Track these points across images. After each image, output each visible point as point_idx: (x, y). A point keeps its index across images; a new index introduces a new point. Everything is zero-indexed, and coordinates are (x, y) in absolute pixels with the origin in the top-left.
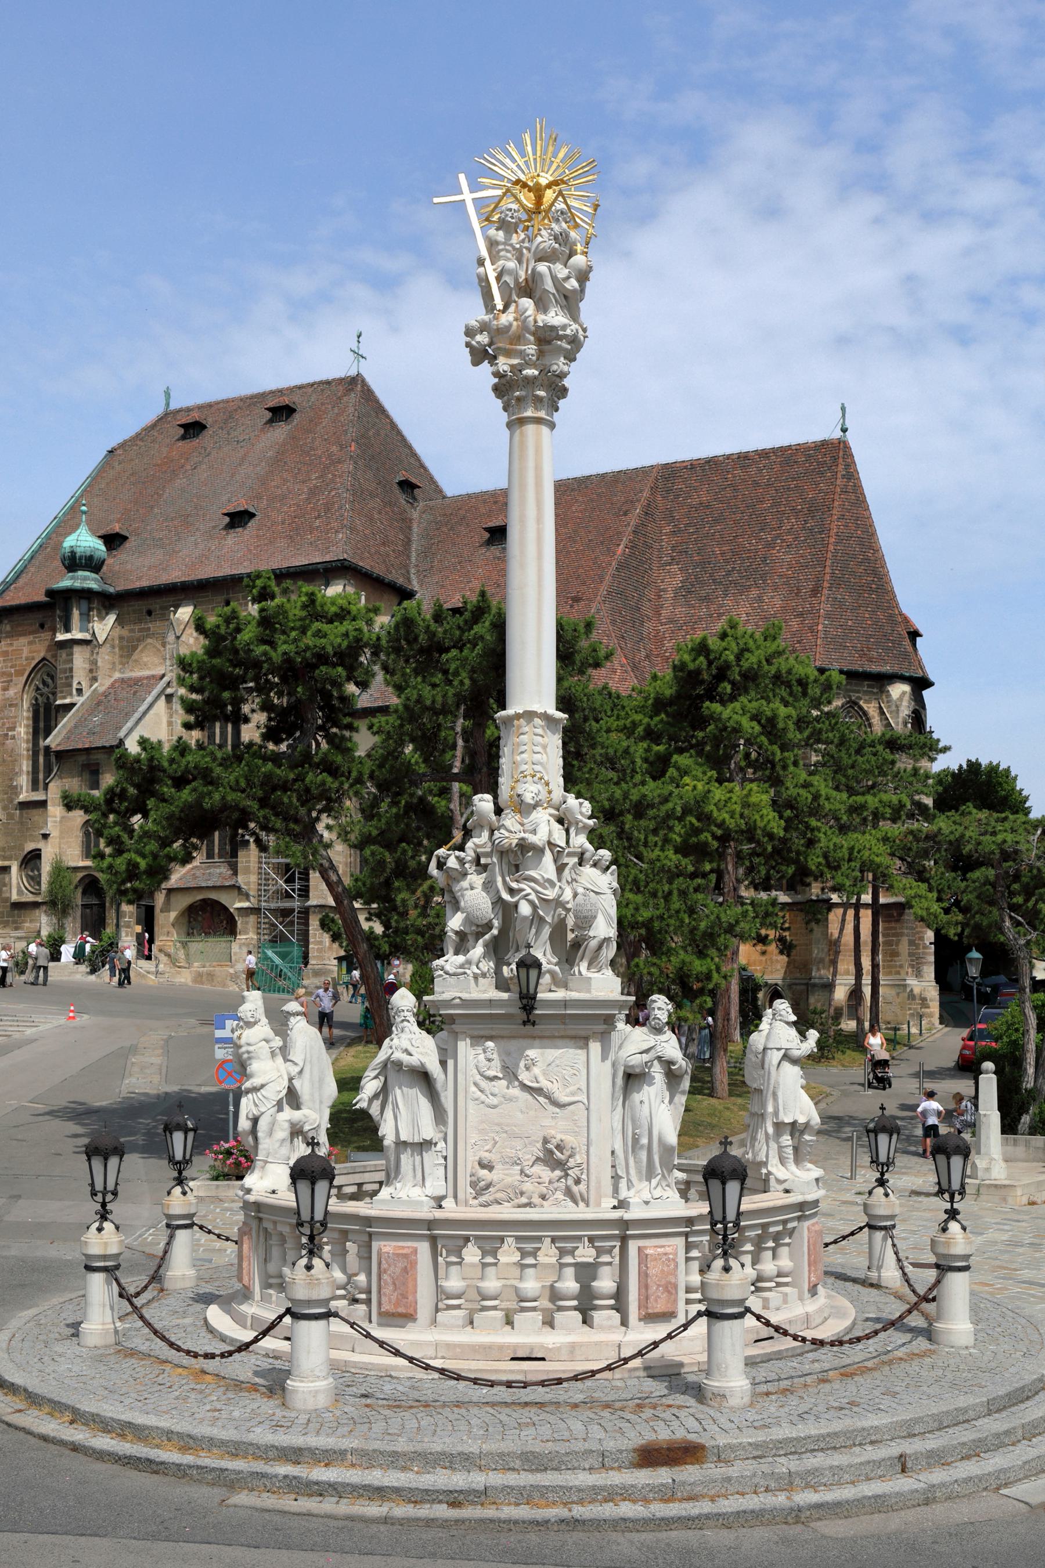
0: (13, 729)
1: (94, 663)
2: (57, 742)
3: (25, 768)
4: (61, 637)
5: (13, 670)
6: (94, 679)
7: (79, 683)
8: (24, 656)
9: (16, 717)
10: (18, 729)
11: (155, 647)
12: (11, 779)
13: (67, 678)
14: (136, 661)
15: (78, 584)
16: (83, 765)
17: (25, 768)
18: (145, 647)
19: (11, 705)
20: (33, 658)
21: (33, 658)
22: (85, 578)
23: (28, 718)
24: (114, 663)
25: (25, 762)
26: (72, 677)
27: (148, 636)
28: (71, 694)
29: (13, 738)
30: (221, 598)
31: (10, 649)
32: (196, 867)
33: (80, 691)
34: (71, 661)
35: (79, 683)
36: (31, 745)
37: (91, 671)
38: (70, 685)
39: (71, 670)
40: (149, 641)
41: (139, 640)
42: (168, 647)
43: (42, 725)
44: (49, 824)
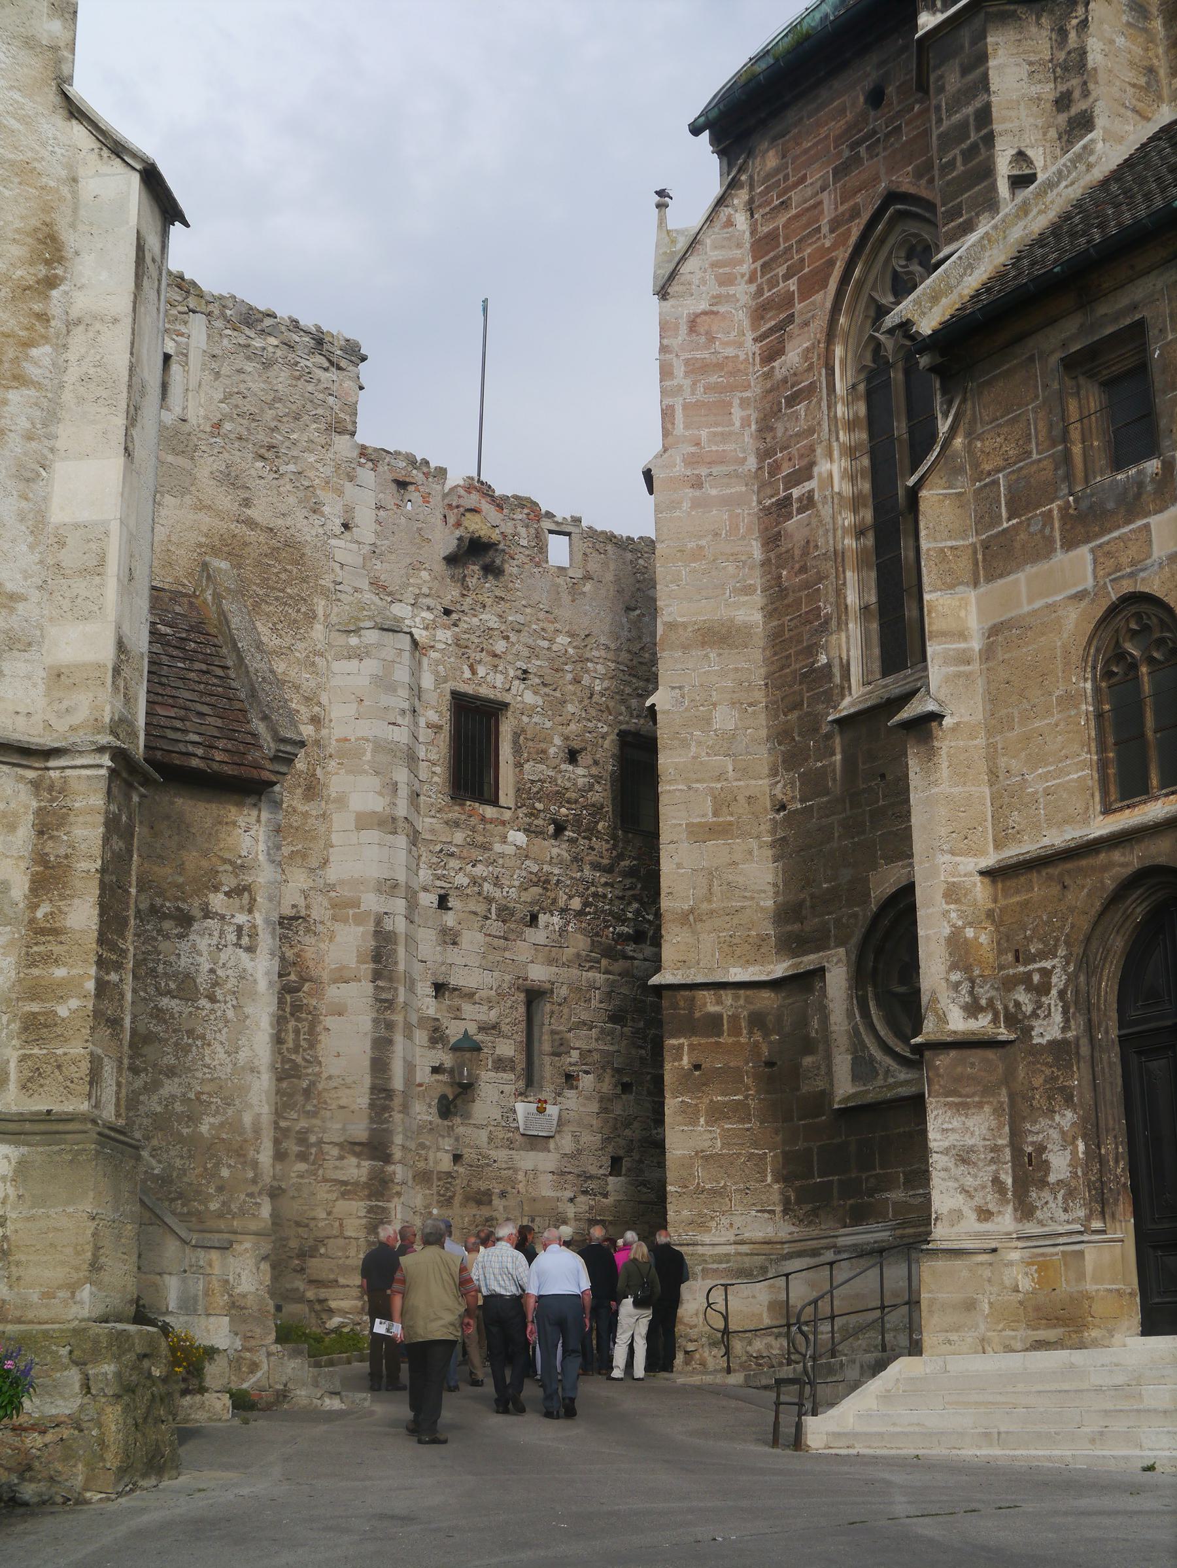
0: (805, 473)
1: (1077, 64)
3: (852, 598)
4: (927, 21)
5: (792, 285)
6: (1085, 123)
7: (1021, 156)
8: (824, 222)
9: (811, 431)
10: (823, 467)
12: (811, 651)
16: (1071, 364)
17: (852, 598)
19: (792, 401)
21: (855, 213)
23: (851, 425)
24: (1151, 70)
25: (851, 576)
26: (989, 140)
28: (990, 204)
29: (808, 502)
31: (782, 220)
34: (984, 84)
35: (1021, 156)
36: (868, 515)
37: (1063, 102)
38: (987, 172)
39: (984, 116)
43: (900, 428)
44: (937, 673)
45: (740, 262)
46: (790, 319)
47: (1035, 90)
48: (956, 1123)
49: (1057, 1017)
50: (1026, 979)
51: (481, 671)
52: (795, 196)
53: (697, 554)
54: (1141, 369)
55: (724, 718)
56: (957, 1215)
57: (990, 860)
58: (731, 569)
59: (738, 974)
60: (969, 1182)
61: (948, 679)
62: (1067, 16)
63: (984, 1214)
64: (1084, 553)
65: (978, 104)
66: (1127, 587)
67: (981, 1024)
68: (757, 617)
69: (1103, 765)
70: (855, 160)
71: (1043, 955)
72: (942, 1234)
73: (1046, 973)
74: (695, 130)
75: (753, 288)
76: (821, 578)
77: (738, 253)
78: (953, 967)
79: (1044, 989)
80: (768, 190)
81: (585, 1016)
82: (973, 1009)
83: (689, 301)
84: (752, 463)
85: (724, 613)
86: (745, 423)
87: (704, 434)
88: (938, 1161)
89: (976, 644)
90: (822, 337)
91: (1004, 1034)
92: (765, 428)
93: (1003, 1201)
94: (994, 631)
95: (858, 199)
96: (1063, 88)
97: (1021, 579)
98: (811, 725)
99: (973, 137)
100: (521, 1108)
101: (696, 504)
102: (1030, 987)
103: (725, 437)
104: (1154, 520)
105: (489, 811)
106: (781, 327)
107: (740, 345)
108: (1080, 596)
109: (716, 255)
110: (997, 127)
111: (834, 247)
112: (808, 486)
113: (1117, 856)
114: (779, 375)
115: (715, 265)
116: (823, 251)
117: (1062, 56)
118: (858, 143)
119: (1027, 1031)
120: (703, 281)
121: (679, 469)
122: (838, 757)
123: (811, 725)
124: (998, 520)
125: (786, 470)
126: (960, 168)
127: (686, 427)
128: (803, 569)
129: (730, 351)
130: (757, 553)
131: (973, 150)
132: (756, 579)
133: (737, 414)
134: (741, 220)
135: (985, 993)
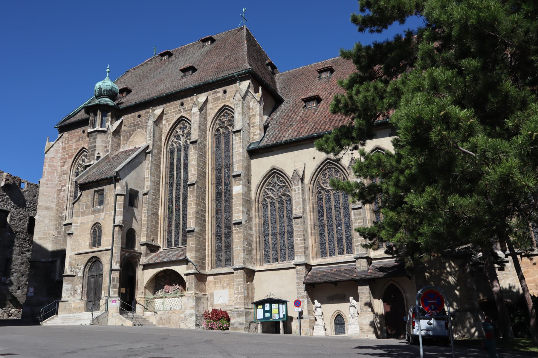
0: (64, 186)
2: (81, 180)
5: (67, 156)
9: (66, 180)
10: (67, 186)
11: (142, 133)
12: (61, 213)
13: (92, 151)
14: (131, 142)
15: (102, 103)
18: (136, 134)
19: (64, 174)
20: (78, 149)
22: (106, 101)
26: (95, 150)
27: (138, 128)
29: (64, 190)
30: (178, 102)
31: (67, 145)
32: (161, 252)
33: (98, 157)
34: (95, 142)
35: (99, 153)
38: (94, 155)
39: (95, 146)
40: (139, 130)
41: (133, 131)
42: (148, 128)
45: (60, 150)
47: (102, 144)
48: (67, 285)
49: (81, 273)
50: (78, 268)
51: (6, 206)
52: (70, 142)
53: (46, 195)
54: (103, 194)
55: (47, 221)
56: (65, 297)
57: (76, 252)
58: (51, 198)
59: (43, 260)
60: (67, 293)
61: (74, 229)
62: (108, 135)
63: (69, 297)
65: (94, 144)
66: (97, 221)
67: (72, 273)
68: (54, 206)
69: (91, 243)
70: (79, 140)
71: (81, 265)
72: (63, 299)
73: (81, 267)
75: (61, 155)
76: (64, 202)
77: (59, 148)
78: (69, 266)
79: (80, 269)
80: (66, 140)
81: (17, 263)
82: (71, 271)
83: (50, 155)
84: (57, 182)
85: (49, 205)
86: (57, 176)
87: (50, 176)
88: (63, 290)
89: (79, 224)
90: (70, 166)
91: (74, 275)
92: (60, 177)
93: (72, 295)
94: (81, 223)
95: (79, 146)
96: (106, 145)
97: (85, 217)
98: (60, 224)
99: (93, 149)
100: (3, 278)
101: (47, 187)
102: (79, 269)
103: (53, 177)
104: (101, 214)
105: (4, 229)
106: (64, 162)
107: (58, 163)
108: (92, 221)
109: (56, 148)
110: (96, 149)
111: (74, 153)
112: (65, 188)
113: (91, 254)
114: (63, 169)
115: (55, 150)
116: (72, 153)
117: (106, 141)
118: (80, 138)
119: (77, 274)
120: (53, 152)
121: (45, 181)
122: (63, 230)
123: (60, 224)
124: (83, 209)
125: (62, 185)
126: (91, 153)
127: (47, 175)
128: (62, 200)
129: (56, 164)
130: (56, 196)
131: (92, 151)
132: (55, 200)
133: (55, 174)
134: (61, 144)
135: (73, 269)
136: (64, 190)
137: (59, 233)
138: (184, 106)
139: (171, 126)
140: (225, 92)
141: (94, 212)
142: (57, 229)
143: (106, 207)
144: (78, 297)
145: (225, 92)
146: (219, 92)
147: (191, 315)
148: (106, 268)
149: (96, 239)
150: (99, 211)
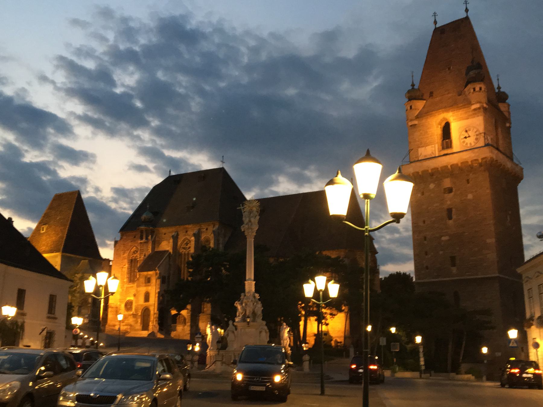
0: (125, 265)
12: (124, 280)
29: (125, 268)
46: (125, 252)
64: (145, 288)
74: (119, 232)
125: (123, 265)
136: (125, 268)
137: (123, 290)
138: (188, 233)
139: (181, 241)
140: (207, 229)
141: (146, 286)
142: (121, 288)
143: (152, 284)
144: (139, 324)
145: (207, 229)
146: (204, 228)
147: (188, 334)
148: (152, 312)
149: (147, 298)
150: (149, 286)
